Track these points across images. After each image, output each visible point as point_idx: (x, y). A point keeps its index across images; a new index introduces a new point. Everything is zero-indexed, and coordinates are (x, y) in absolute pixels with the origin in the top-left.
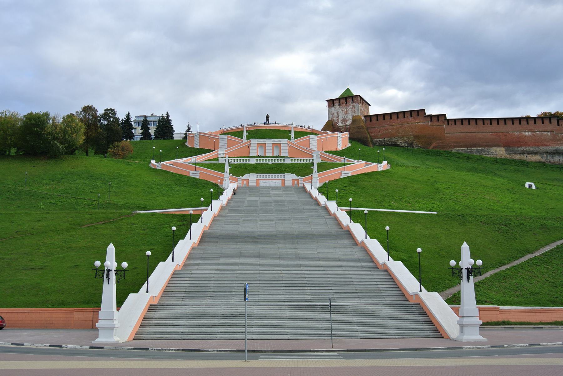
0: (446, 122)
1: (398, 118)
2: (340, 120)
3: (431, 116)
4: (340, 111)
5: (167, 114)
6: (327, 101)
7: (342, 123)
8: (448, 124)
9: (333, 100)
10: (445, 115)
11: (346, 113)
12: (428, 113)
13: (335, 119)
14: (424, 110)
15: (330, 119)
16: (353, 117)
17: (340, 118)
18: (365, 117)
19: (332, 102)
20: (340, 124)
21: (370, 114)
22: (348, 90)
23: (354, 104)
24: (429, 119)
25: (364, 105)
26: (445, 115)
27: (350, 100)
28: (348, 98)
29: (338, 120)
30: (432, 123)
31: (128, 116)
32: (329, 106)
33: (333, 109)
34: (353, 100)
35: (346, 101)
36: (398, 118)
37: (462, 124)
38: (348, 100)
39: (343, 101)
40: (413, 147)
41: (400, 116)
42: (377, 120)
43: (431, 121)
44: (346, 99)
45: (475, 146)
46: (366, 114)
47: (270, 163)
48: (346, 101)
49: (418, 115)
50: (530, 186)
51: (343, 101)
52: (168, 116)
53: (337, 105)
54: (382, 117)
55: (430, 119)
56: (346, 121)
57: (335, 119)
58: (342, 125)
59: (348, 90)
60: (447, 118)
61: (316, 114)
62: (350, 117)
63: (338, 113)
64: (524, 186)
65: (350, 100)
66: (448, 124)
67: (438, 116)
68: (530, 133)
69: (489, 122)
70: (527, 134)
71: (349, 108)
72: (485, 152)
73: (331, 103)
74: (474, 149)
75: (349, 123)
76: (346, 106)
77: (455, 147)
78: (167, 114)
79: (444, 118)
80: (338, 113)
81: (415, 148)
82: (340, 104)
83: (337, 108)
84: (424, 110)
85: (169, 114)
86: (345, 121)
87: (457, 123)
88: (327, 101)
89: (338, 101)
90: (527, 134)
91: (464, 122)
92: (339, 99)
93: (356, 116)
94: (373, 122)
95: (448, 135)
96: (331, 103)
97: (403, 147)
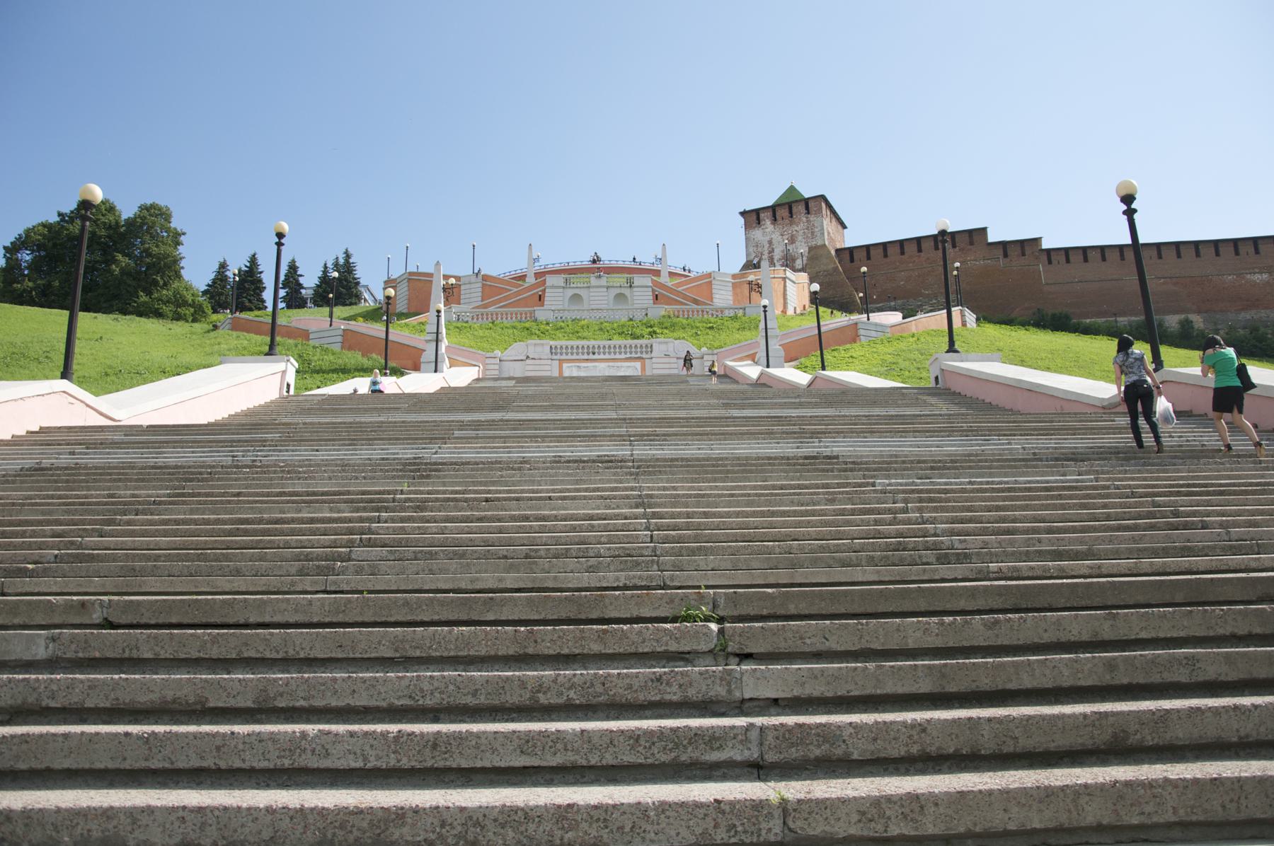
0: (1044, 258)
1: (920, 250)
3: (1004, 245)
4: (776, 237)
5: (346, 253)
6: (743, 214)
8: (1050, 262)
9: (757, 212)
11: (792, 240)
12: (992, 238)
14: (984, 230)
16: (811, 249)
18: (837, 251)
23: (812, 218)
24: (1000, 252)
26: (1036, 241)
27: (801, 208)
28: (793, 207)
30: (1008, 260)
31: (253, 260)
32: (748, 226)
33: (757, 234)
34: (807, 208)
35: (791, 212)
36: (920, 250)
38: (794, 209)
39: (782, 212)
41: (924, 245)
43: (1006, 255)
44: (790, 206)
45: (1124, 314)
46: (838, 246)
48: (791, 212)
49: (972, 243)
51: (782, 212)
52: (348, 256)
54: (881, 250)
55: (1001, 252)
60: (1045, 246)
61: (711, 246)
63: (770, 242)
66: (1050, 262)
67: (1022, 243)
68: (1265, 276)
69: (1154, 253)
70: (1257, 278)
71: (799, 228)
73: (753, 218)
78: (346, 253)
80: (770, 242)
82: (775, 219)
84: (984, 230)
85: (351, 251)
87: (1071, 258)
88: (743, 214)
89: (769, 214)
90: (1257, 278)
91: (1090, 254)
92: (773, 209)
93: (817, 247)
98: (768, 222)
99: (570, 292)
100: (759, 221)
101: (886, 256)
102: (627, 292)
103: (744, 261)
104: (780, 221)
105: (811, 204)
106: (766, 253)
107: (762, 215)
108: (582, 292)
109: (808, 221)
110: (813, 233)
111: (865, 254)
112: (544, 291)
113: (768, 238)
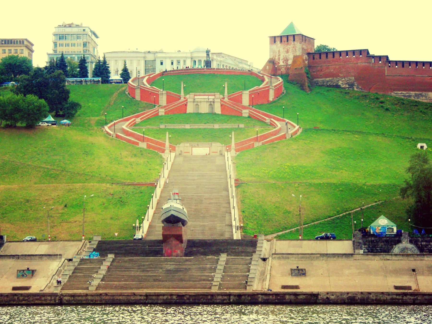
4: (281, 49)
7: (283, 62)
9: (275, 37)
10: (387, 57)
11: (287, 52)
13: (277, 58)
15: (272, 57)
17: (281, 57)
18: (309, 54)
19: (273, 39)
20: (281, 63)
23: (295, 43)
25: (307, 42)
29: (279, 59)
32: (271, 43)
33: (274, 46)
37: (403, 67)
38: (289, 38)
39: (284, 39)
40: (353, 88)
42: (320, 58)
50: (422, 147)
53: (278, 42)
54: (325, 55)
56: (287, 60)
57: (277, 58)
58: (283, 64)
62: (291, 56)
63: (279, 51)
64: (416, 146)
71: (290, 47)
72: (422, 96)
73: (274, 39)
74: (413, 93)
75: (290, 62)
76: (288, 44)
77: (395, 90)
79: (385, 60)
80: (279, 51)
81: (355, 89)
82: (281, 41)
83: (279, 46)
89: (279, 39)
94: (315, 60)
95: (388, 77)
97: (344, 88)
99: (195, 103)
100: (275, 42)
102: (212, 103)
103: (267, 58)
104: (283, 42)
105: (296, 37)
106: (277, 55)
107: (276, 39)
108: (199, 104)
109: (294, 44)
110: (295, 50)
111: (319, 56)
112: (187, 103)
113: (278, 50)
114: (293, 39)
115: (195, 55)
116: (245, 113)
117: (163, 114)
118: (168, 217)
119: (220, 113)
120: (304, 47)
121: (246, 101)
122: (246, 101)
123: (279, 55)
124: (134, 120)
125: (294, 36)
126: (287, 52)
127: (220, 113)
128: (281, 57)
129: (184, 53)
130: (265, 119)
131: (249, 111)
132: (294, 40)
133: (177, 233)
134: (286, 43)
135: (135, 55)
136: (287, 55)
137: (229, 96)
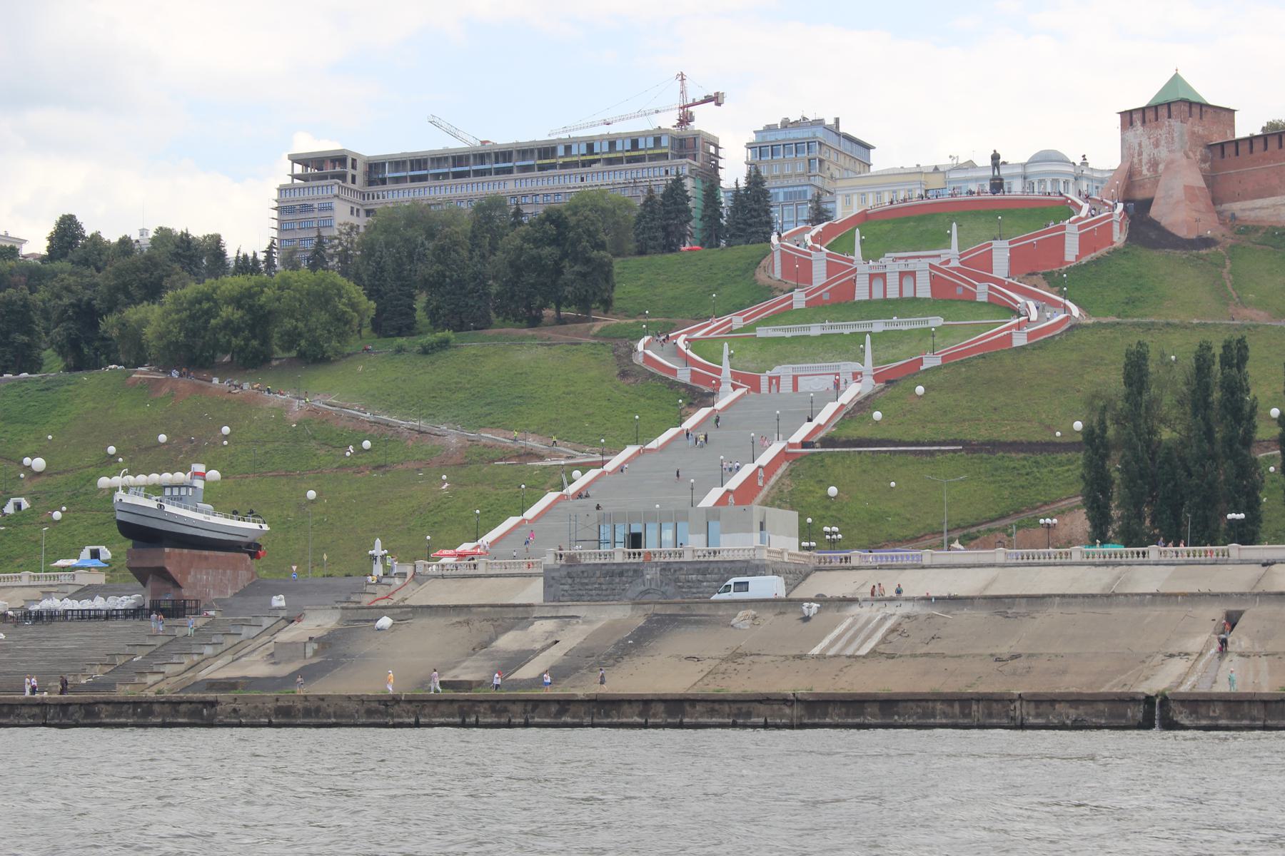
2: (1144, 161)
4: (1145, 142)
9: (1131, 112)
11: (1157, 145)
13: (1136, 160)
17: (1145, 157)
21: (1238, 135)
22: (1176, 80)
23: (1172, 121)
27: (1163, 112)
29: (1140, 161)
33: (1130, 134)
47: (847, 331)
59: (1176, 80)
63: (1140, 145)
65: (1163, 112)
73: (1128, 118)
80: (1140, 145)
82: (1144, 122)
86: (1154, 164)
92: (1143, 110)
96: (1128, 118)
98: (1139, 123)
100: (1131, 124)
101: (1251, 151)
104: (1148, 124)
105: (1173, 108)
113: (1137, 141)
114: (1166, 114)
115: (1031, 170)
116: (982, 292)
117: (803, 306)
118: (729, 533)
119: (929, 295)
120: (1199, 129)
121: (1001, 267)
122: (1001, 267)
123: (1140, 154)
124: (730, 321)
125: (1169, 104)
126: (1157, 145)
127: (929, 295)
128: (1145, 157)
129: (1014, 166)
130: (1017, 302)
131: (991, 288)
132: (1170, 117)
133: (157, 564)
134: (1154, 124)
135: (917, 177)
136: (1155, 151)
137: (961, 256)
